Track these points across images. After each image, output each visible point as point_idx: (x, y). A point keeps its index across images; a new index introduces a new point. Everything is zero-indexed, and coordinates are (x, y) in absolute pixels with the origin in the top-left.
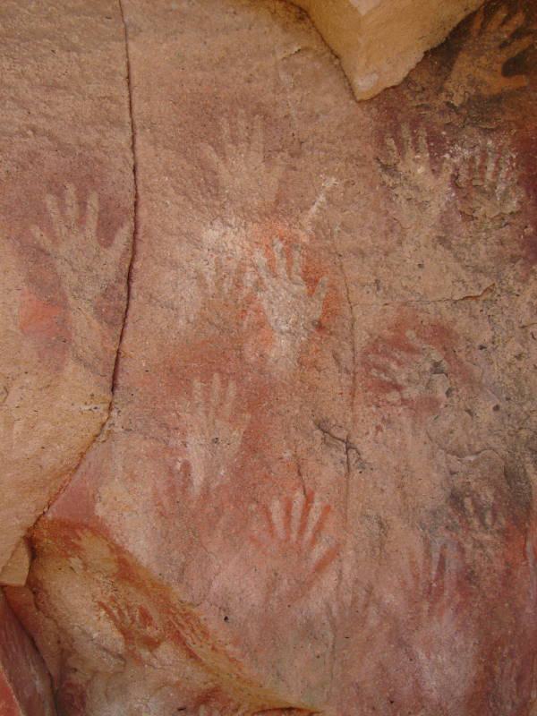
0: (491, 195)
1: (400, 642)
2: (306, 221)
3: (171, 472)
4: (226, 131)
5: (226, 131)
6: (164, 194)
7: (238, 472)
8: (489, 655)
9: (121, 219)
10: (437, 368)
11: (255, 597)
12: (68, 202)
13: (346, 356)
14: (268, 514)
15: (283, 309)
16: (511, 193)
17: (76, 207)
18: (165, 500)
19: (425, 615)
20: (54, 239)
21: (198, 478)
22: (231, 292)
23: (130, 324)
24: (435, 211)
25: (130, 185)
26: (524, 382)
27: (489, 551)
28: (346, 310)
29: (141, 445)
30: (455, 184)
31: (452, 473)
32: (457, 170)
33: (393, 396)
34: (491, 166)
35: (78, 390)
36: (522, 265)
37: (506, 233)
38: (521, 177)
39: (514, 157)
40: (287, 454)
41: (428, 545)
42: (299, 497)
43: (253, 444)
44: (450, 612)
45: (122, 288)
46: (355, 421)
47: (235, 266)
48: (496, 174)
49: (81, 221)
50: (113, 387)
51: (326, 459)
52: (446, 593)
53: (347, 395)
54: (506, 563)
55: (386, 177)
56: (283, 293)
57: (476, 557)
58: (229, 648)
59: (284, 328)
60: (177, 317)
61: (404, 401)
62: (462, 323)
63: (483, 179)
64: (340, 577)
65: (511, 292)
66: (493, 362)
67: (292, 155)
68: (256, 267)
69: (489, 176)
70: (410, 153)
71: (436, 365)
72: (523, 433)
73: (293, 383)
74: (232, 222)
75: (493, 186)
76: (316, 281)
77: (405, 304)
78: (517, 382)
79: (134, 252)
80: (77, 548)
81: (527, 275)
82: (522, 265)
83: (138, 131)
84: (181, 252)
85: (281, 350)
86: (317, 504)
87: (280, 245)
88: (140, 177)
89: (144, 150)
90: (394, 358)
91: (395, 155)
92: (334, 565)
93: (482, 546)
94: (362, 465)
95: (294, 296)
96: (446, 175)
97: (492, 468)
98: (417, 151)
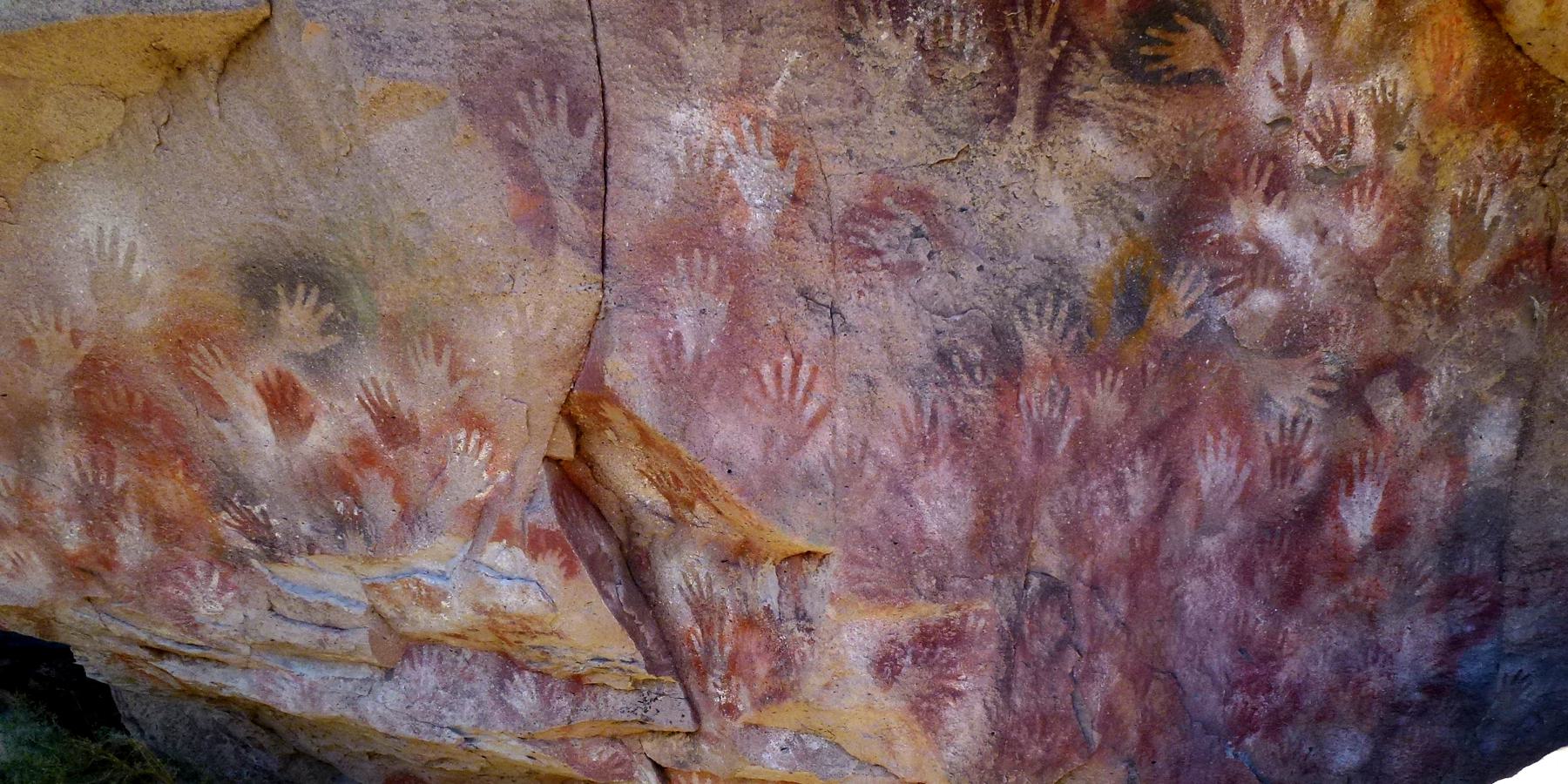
0: (959, 56)
1: (899, 490)
2: (771, 97)
3: (663, 343)
4: (684, 14)
5: (684, 14)
6: (629, 82)
7: (726, 339)
8: (988, 501)
9: (590, 110)
10: (917, 233)
11: (755, 452)
12: (538, 97)
13: (824, 226)
14: (760, 377)
15: (756, 184)
16: (980, 51)
17: (546, 102)
18: (661, 367)
19: (921, 466)
20: (527, 129)
21: (690, 346)
22: (703, 171)
23: (609, 208)
24: (903, 77)
25: (596, 77)
27: (981, 404)
28: (820, 181)
29: (635, 319)
30: (920, 45)
31: (938, 332)
32: (922, 32)
33: (873, 262)
34: (957, 25)
35: (571, 274)
37: (978, 93)
38: (991, 34)
40: (772, 321)
41: (918, 401)
42: (787, 360)
43: (739, 313)
44: (945, 463)
45: (598, 175)
46: (838, 287)
47: (705, 146)
48: (963, 34)
49: (552, 115)
50: (603, 267)
51: (811, 323)
52: (941, 445)
53: (827, 264)
54: (1000, 416)
55: (849, 47)
56: (755, 168)
57: (968, 410)
58: (736, 497)
59: (759, 202)
60: (653, 198)
61: (884, 266)
62: (939, 187)
63: (949, 40)
64: (834, 432)
67: (752, 33)
68: (726, 146)
69: (955, 36)
70: (872, 20)
71: (916, 229)
72: (1011, 292)
73: (772, 254)
74: (698, 103)
75: (961, 46)
76: (787, 155)
77: (880, 172)
78: (1000, 242)
79: (606, 140)
80: (606, 420)
83: (598, 23)
84: (651, 136)
85: (758, 221)
86: (805, 365)
87: (748, 122)
88: (604, 66)
89: (606, 40)
90: (872, 225)
91: (857, 23)
92: (828, 420)
93: (973, 401)
94: (848, 329)
95: (766, 171)
96: (911, 38)
97: (978, 327)
98: (879, 15)
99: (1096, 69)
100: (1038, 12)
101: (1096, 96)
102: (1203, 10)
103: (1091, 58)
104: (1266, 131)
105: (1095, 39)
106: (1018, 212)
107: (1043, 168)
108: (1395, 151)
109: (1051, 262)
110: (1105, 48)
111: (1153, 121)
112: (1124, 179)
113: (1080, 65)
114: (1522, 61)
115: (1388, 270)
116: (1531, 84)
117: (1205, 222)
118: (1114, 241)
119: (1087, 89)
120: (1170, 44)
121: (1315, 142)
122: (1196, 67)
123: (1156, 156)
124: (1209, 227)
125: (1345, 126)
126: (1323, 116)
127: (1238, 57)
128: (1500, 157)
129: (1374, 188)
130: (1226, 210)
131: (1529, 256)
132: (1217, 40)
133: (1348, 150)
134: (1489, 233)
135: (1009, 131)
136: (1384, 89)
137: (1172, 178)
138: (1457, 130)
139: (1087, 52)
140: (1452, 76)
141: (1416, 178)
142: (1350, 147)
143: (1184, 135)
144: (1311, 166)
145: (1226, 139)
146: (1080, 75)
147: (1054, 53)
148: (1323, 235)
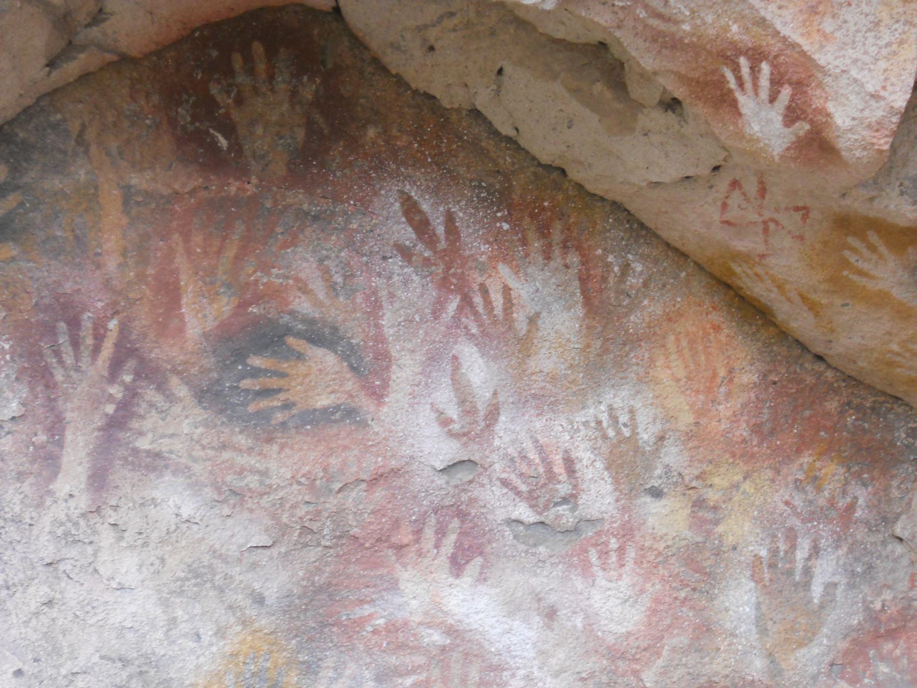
26: (61, 636)
36: (31, 485)
38: (22, 371)
39: (7, 347)
65: (21, 521)
66: (11, 614)
81: (41, 497)
82: (31, 485)
99: (177, 409)
100: (90, 341)
101: (178, 445)
102: (327, 331)
103: (171, 398)
104: (440, 481)
105: (174, 371)
106: (72, 593)
107: (107, 537)
108: (648, 499)
109: (125, 662)
110: (187, 382)
111: (264, 474)
112: (232, 550)
113: (152, 405)
114: (829, 374)
115: (660, 662)
116: (849, 403)
117: (361, 602)
118: (220, 633)
119: (163, 436)
120: (283, 375)
121: (518, 493)
122: (323, 401)
123: (274, 517)
124: (367, 610)
125: (559, 469)
126: (524, 457)
127: (385, 385)
128: (822, 502)
129: (621, 550)
130: (393, 586)
131: (892, 635)
132: (353, 369)
133: (570, 499)
134: (822, 607)
135: (50, 493)
136: (614, 419)
137: (306, 545)
138: (743, 467)
139: (161, 387)
140: (721, 397)
141: (688, 534)
142: (574, 496)
143: (312, 486)
144: (519, 522)
145: (379, 494)
146: (151, 421)
147: (116, 391)
148: (551, 614)
